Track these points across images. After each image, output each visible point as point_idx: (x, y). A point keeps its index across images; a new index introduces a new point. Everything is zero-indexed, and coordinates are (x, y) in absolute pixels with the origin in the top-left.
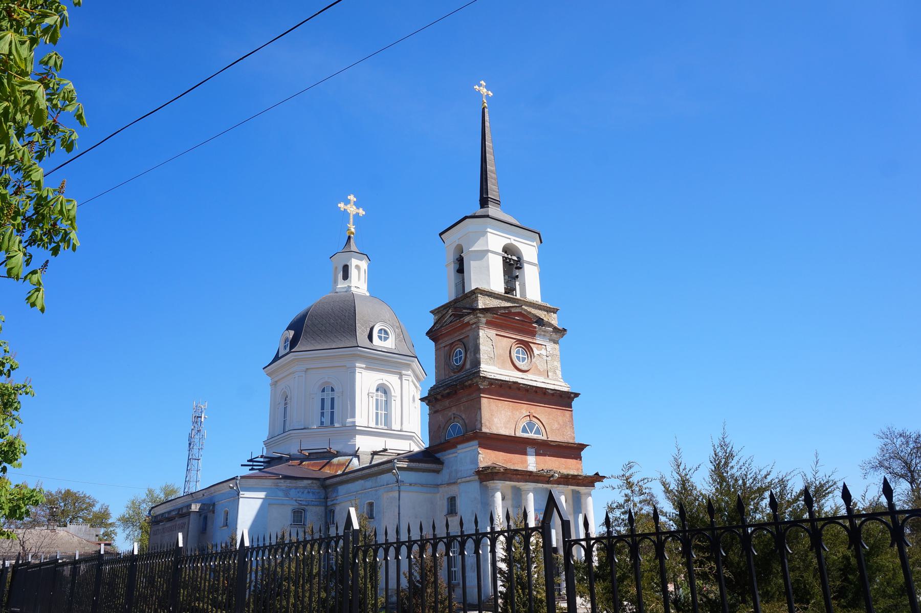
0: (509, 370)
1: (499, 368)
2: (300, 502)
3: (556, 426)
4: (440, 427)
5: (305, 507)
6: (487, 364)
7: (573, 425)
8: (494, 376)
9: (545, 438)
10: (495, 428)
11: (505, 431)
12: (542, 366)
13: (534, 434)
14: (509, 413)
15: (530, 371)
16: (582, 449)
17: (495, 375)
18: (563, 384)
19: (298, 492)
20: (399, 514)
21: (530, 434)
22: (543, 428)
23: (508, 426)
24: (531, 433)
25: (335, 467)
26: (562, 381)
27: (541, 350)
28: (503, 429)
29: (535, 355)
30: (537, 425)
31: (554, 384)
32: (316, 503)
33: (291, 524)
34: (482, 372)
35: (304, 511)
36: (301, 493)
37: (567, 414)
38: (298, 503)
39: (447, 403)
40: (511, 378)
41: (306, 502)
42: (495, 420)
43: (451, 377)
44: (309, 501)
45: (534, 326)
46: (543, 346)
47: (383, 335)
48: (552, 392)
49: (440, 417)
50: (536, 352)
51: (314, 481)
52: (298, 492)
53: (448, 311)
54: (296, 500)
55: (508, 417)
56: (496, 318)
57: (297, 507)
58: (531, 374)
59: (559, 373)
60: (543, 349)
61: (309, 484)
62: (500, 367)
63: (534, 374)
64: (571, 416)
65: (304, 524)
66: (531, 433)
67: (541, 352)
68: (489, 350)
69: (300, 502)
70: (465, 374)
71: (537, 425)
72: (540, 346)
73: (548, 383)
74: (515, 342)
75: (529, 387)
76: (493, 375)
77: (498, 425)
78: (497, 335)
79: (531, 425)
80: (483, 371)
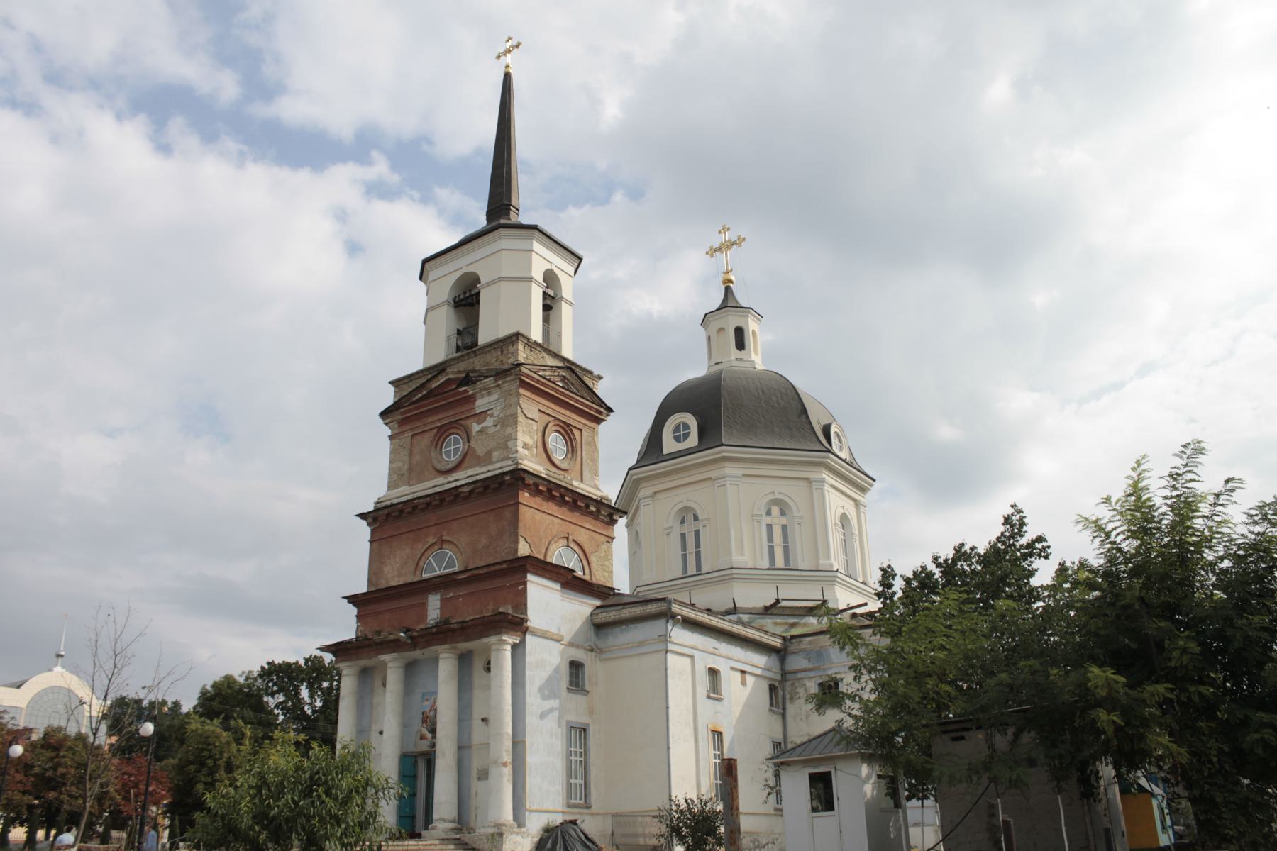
3: (484, 541)
12: (480, 450)
13: (444, 569)
14: (408, 551)
24: (440, 570)
27: (485, 420)
31: (489, 471)
47: (682, 433)
48: (466, 489)
50: (476, 427)
55: (405, 557)
56: (405, 412)
63: (467, 468)
66: (440, 570)
67: (484, 424)
68: (401, 464)
72: (482, 416)
75: (428, 499)
77: (389, 576)
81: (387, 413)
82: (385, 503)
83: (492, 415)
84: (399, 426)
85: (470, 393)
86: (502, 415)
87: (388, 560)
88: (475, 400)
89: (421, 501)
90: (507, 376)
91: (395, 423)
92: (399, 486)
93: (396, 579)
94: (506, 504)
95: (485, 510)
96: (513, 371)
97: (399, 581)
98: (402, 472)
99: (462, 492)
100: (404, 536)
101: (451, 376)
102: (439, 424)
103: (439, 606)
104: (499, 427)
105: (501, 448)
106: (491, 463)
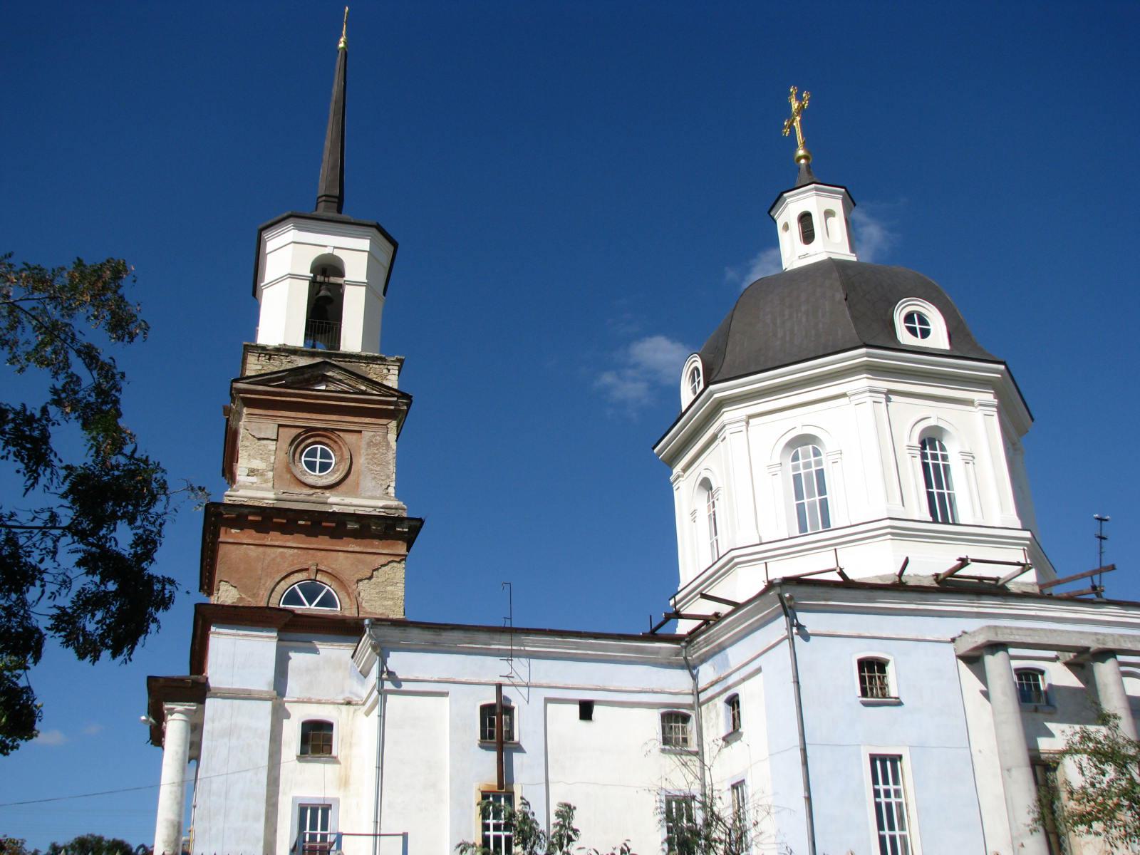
13: (316, 606)
21: (308, 606)
24: (310, 604)
66: (310, 604)
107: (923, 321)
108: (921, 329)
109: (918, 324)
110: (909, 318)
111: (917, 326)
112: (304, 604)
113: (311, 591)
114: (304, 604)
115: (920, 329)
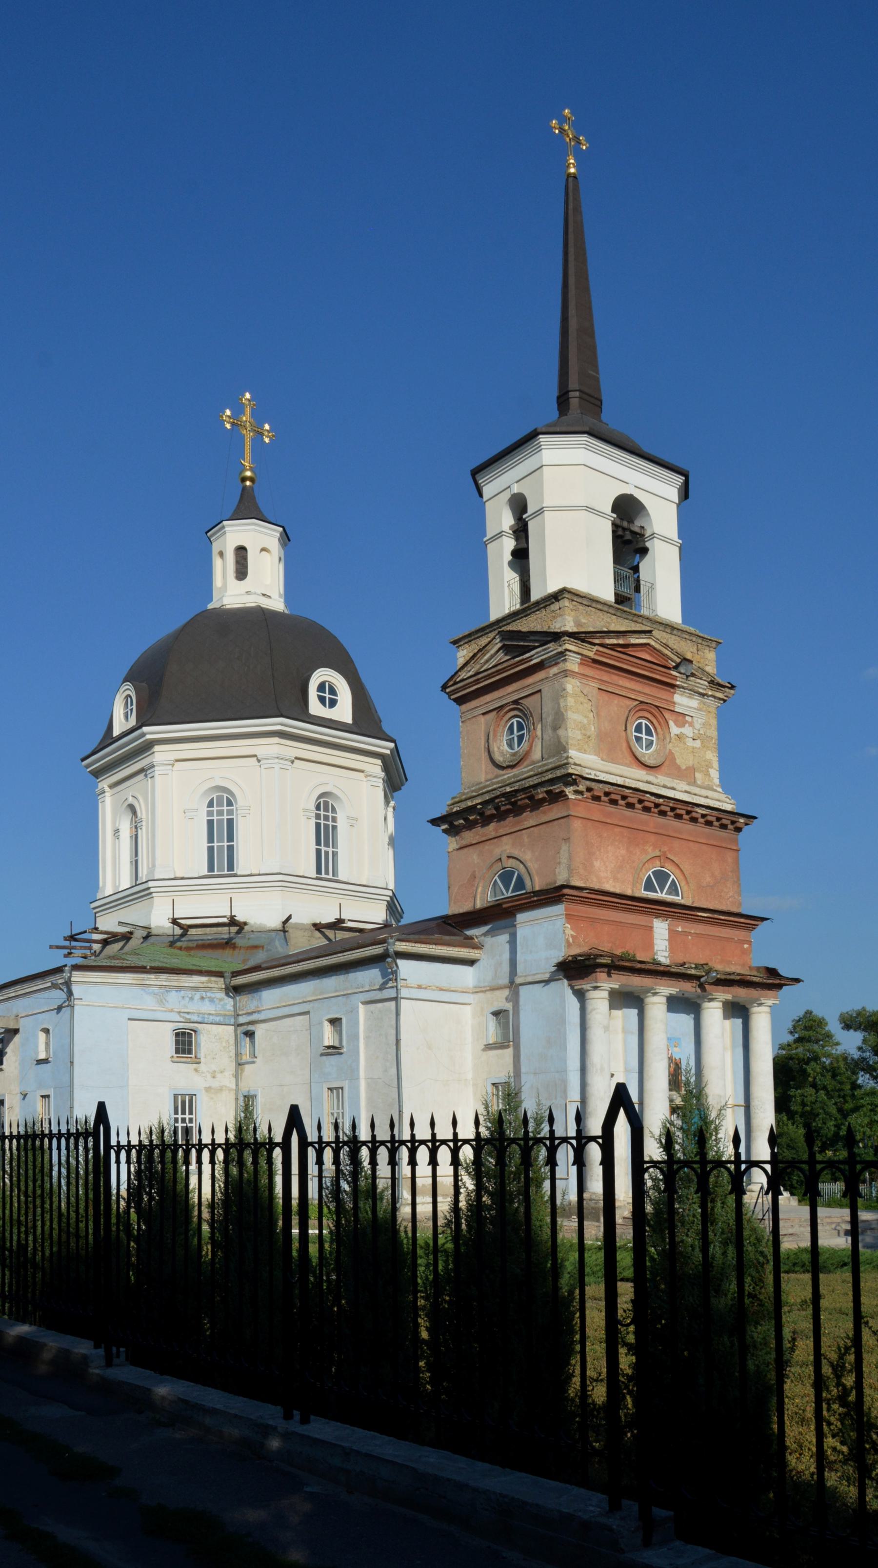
0: (622, 764)
1: (602, 760)
2: (188, 1016)
3: (708, 879)
4: (474, 877)
5: (196, 1025)
6: (580, 750)
7: (738, 879)
8: (597, 776)
9: (688, 902)
10: (595, 880)
11: (614, 887)
12: (683, 760)
14: (623, 852)
15: (663, 768)
16: (753, 927)
17: (598, 773)
18: (723, 797)
19: (183, 997)
20: (398, 1042)
22: (683, 883)
23: (619, 876)
24: (662, 893)
25: (242, 951)
26: (720, 790)
28: (611, 882)
29: (672, 735)
30: (672, 876)
31: (707, 797)
32: (217, 1019)
33: (173, 1057)
34: (573, 767)
35: (195, 1031)
36: (187, 999)
37: (729, 856)
38: (183, 1017)
39: (491, 829)
40: (627, 780)
41: (198, 1016)
42: (595, 863)
43: (497, 777)
44: (204, 1014)
45: (671, 675)
46: (688, 718)
49: (475, 857)
50: (675, 730)
51: (213, 979)
52: (183, 997)
53: (494, 638)
54: (179, 1013)
55: (621, 858)
57: (181, 1025)
58: (662, 775)
59: (715, 774)
60: (687, 725)
61: (203, 983)
62: (604, 757)
63: (668, 775)
64: (737, 861)
65: (196, 1057)
66: (662, 893)
68: (585, 721)
69: (188, 1016)
70: (531, 770)
71: (672, 876)
72: (681, 718)
73: (695, 795)
74: (635, 706)
75: (661, 800)
76: (593, 772)
78: (599, 689)
79: (662, 877)
80: (575, 764)
81: (575, 638)
82: (587, 771)
83: (691, 724)
84: (581, 664)
85: (678, 683)
86: (702, 732)
87: (598, 853)
88: (675, 693)
89: (653, 798)
90: (718, 690)
91: (579, 657)
92: (585, 752)
93: (611, 882)
94: (729, 846)
95: (715, 843)
96: (727, 690)
97: (614, 887)
98: (588, 734)
99: (697, 812)
100: (617, 829)
101: (653, 643)
102: (641, 699)
103: (667, 937)
104: (698, 744)
105: (702, 771)
106: (694, 783)
107: (333, 691)
108: (330, 699)
109: (329, 697)
110: (321, 687)
111: (327, 695)
112: (657, 892)
113: (662, 877)
114: (657, 892)
115: (329, 698)
